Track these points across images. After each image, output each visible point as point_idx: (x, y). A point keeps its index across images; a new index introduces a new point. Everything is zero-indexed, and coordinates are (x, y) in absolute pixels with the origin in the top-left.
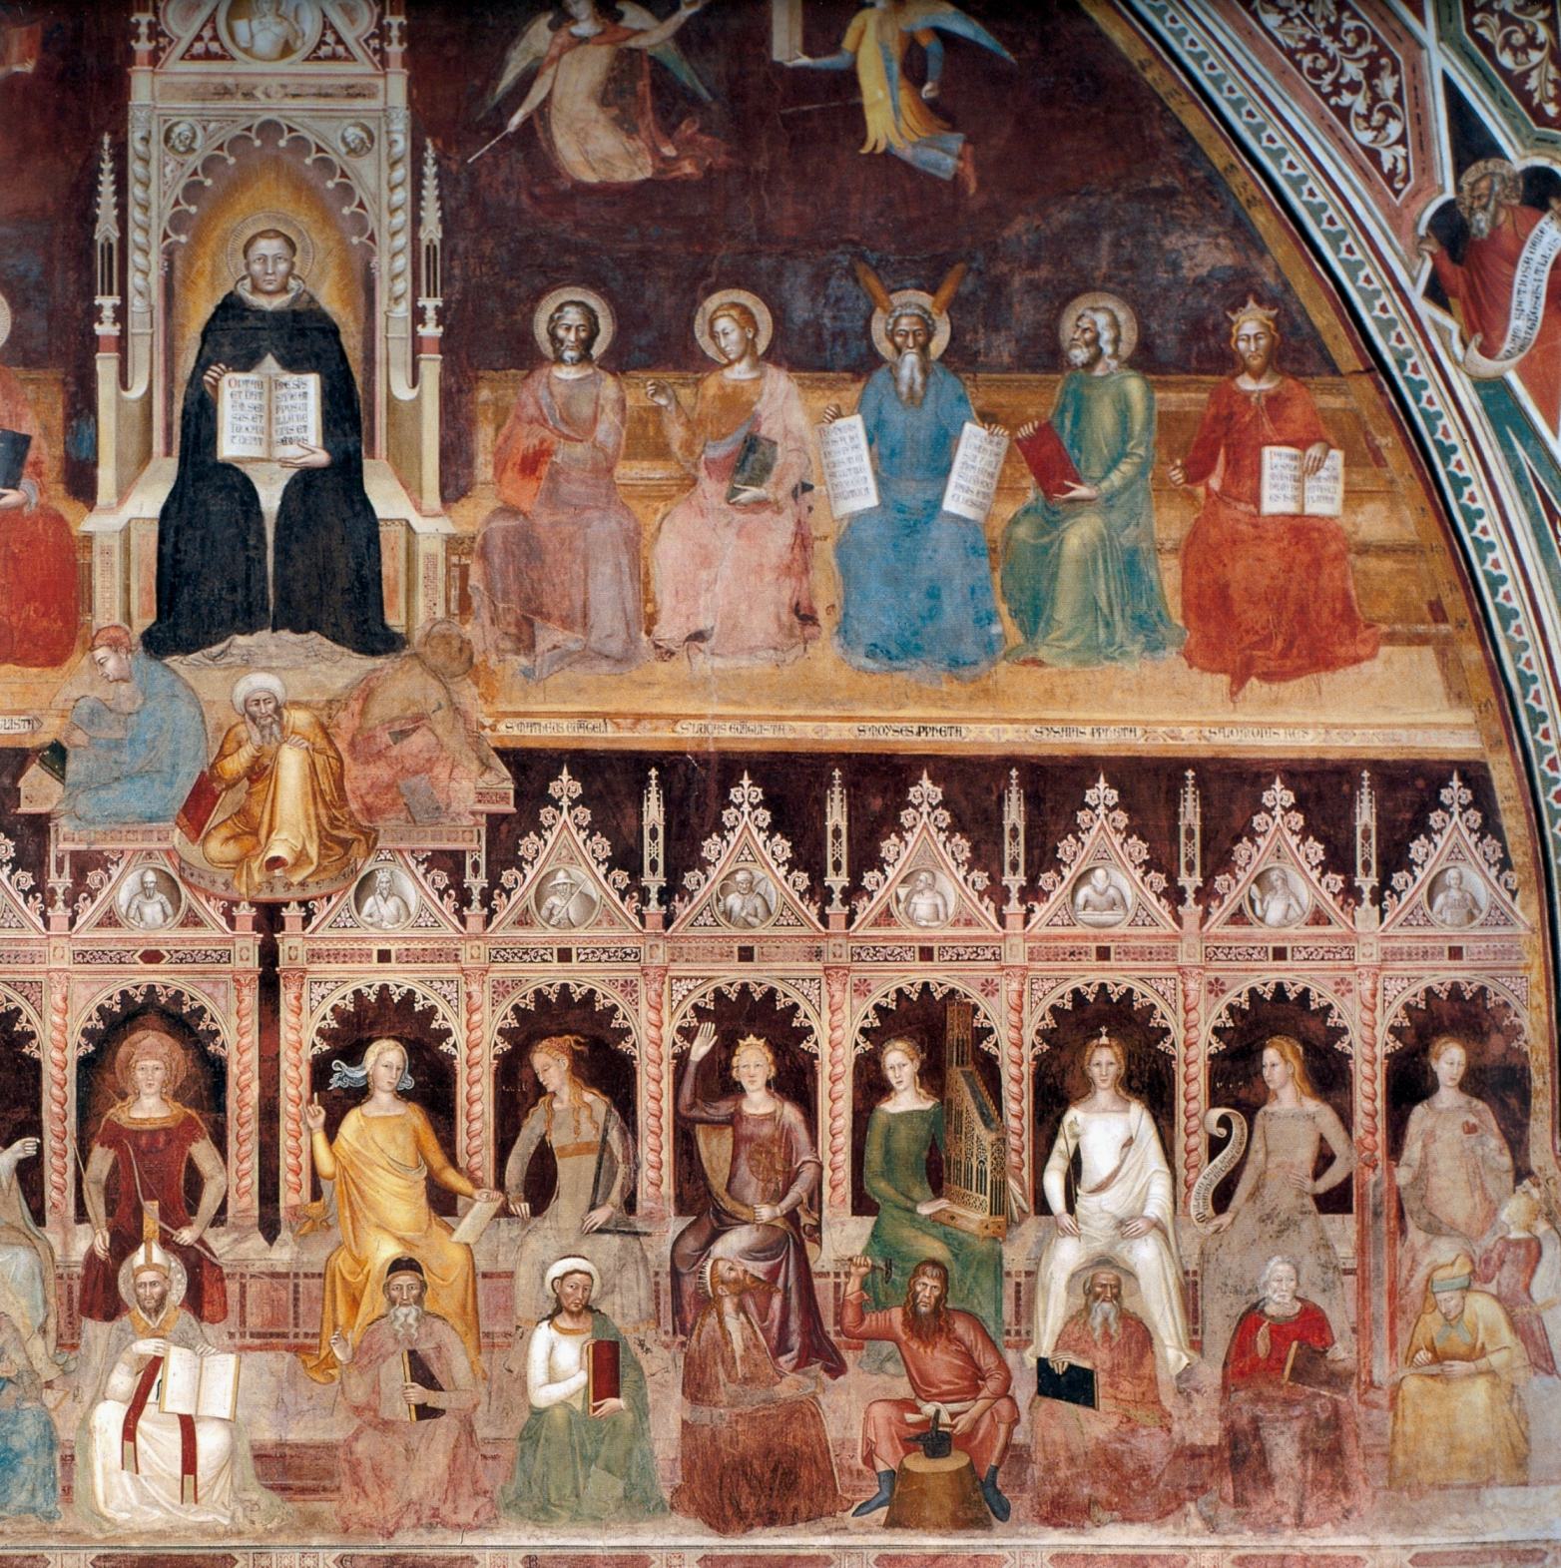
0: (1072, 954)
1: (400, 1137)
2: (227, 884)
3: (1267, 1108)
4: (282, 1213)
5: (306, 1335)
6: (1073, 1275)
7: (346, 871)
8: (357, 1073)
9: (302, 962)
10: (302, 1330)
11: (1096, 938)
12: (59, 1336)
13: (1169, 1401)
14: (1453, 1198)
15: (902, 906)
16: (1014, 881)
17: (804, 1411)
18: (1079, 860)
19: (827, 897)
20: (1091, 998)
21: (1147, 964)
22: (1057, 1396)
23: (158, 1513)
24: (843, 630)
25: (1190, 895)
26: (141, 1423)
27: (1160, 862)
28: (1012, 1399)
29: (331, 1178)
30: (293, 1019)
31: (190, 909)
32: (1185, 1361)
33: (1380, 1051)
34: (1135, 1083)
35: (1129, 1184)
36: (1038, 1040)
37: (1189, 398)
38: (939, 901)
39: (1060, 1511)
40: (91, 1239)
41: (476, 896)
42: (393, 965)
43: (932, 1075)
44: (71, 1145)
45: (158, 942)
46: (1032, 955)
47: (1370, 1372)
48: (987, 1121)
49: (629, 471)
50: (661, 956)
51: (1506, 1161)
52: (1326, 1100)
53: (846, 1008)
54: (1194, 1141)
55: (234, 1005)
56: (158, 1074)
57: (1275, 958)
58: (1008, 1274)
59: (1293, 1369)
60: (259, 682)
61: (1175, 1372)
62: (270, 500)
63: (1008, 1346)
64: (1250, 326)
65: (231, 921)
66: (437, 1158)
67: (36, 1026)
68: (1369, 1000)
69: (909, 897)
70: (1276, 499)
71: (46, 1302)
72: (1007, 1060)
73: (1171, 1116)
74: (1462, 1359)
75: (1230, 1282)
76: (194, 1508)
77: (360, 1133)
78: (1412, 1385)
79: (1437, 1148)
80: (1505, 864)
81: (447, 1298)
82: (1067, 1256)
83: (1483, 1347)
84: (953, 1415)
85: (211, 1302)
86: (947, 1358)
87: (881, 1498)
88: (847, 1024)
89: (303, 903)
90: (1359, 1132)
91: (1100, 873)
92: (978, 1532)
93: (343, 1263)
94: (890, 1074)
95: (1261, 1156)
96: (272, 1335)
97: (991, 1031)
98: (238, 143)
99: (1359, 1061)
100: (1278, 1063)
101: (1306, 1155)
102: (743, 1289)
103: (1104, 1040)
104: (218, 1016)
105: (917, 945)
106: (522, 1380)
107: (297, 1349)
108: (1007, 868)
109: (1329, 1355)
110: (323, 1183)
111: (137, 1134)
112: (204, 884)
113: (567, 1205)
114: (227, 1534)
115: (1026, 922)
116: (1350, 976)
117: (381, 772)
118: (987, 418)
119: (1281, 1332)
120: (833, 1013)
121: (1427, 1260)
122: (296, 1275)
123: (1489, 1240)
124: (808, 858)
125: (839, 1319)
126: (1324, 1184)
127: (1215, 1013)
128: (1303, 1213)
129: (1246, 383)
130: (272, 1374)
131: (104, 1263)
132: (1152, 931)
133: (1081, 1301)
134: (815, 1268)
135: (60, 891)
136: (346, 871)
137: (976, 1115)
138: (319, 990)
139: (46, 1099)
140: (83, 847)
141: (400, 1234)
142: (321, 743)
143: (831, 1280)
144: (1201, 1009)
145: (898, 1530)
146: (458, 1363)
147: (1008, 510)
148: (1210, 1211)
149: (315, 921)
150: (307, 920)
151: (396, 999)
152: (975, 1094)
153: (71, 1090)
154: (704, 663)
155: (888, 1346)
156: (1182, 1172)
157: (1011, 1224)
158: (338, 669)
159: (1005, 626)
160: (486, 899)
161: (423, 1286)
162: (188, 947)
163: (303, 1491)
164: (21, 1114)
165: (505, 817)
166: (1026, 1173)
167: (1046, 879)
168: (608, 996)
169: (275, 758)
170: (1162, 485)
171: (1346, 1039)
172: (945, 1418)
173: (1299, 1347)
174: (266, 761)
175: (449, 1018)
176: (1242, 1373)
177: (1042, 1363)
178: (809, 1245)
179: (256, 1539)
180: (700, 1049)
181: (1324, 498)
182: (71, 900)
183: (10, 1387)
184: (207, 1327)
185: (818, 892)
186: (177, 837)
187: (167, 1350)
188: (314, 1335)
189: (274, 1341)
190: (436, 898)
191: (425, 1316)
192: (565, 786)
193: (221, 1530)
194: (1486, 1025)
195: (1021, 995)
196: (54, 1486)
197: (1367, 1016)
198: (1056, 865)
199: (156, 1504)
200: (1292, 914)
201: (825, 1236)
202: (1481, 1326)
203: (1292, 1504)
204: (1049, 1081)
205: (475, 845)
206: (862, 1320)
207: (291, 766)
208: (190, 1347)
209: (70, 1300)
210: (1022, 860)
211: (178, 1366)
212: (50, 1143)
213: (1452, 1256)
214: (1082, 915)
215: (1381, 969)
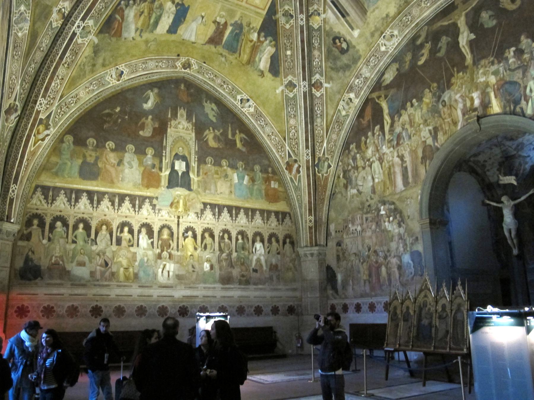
7: (187, 213)
14: (288, 254)
16: (250, 220)
17: (231, 273)
24: (235, 194)
26: (164, 271)
27: (263, 219)
37: (265, 176)
39: (255, 284)
40: (158, 251)
43: (243, 239)
46: (252, 227)
49: (215, 176)
50: (217, 225)
60: (178, 193)
62: (180, 174)
64: (270, 169)
70: (272, 186)
81: (196, 259)
82: (255, 258)
93: (185, 255)
98: (178, 137)
100: (273, 240)
101: (276, 249)
102: (226, 260)
106: (203, 268)
107: (180, 264)
113: (208, 250)
118: (248, 175)
119: (274, 266)
124: (231, 216)
129: (270, 175)
136: (187, 213)
146: (197, 266)
147: (249, 184)
154: (222, 195)
158: (187, 192)
159: (249, 195)
168: (212, 228)
170: (263, 184)
175: (197, 229)
180: (221, 235)
181: (276, 186)
182: (158, 214)
184: (171, 261)
185: (232, 219)
186: (169, 208)
192: (208, 206)
207: (181, 202)
211: (168, 265)
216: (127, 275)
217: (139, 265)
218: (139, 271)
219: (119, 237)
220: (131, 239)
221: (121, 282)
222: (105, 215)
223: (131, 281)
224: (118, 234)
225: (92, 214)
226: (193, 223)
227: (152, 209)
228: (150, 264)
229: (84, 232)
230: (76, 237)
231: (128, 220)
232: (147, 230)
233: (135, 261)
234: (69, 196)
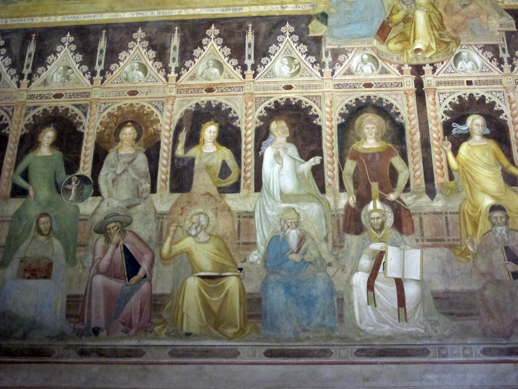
1: (487, 154)
2: (398, 59)
4: (436, 186)
5: (454, 240)
8: (463, 128)
9: (433, 85)
10: (451, 238)
12: (334, 242)
23: (387, 327)
26: (377, 283)
29: (457, 171)
30: (432, 108)
31: (383, 68)
41: (505, 60)
42: (474, 86)
44: (336, 159)
45: (370, 80)
55: (405, 102)
56: (374, 130)
65: (401, 72)
66: (505, 162)
67: (319, 112)
71: (327, 226)
76: (405, 324)
77: (468, 152)
85: (406, 226)
89: (432, 65)
93: (467, 207)
96: (437, 240)
104: (399, 107)
110: (454, 173)
111: (366, 155)
112: (388, 59)
114: (424, 337)
117: (458, 18)
122: (446, 213)
130: (439, 258)
131: (354, 210)
135: (327, 63)
138: (442, 97)
139: (324, 141)
140: (336, 47)
141: (492, 194)
142: (431, 9)
149: (437, 71)
150: (434, 71)
151: (477, 99)
153: (335, 137)
160: (510, 61)
161: (507, 217)
162: (383, 82)
163: (459, 315)
164: (313, 147)
165: (513, 32)
169: (414, 15)
174: (410, 16)
179: (440, 340)
183: (311, 266)
184: (406, 238)
186: (375, 43)
187: (386, 248)
188: (458, 240)
189: (439, 243)
190: (488, 61)
191: (509, 231)
193: (420, 335)
196: (334, 314)
199: (386, 322)
205: (502, 42)
207: (421, 18)
208: (397, 246)
209: (339, 226)
212: (327, 159)
216: (215, 308)
217: (265, 260)
218: (265, 284)
219: (179, 159)
220: (231, 163)
221: (188, 335)
222: (133, 93)
223: (230, 331)
224: (180, 152)
225: (87, 95)
226: (479, 83)
227: (308, 54)
228: (312, 254)
229: (58, 154)
230: (25, 175)
231: (215, 98)
232: (291, 126)
233: (251, 245)
234: (16, 51)
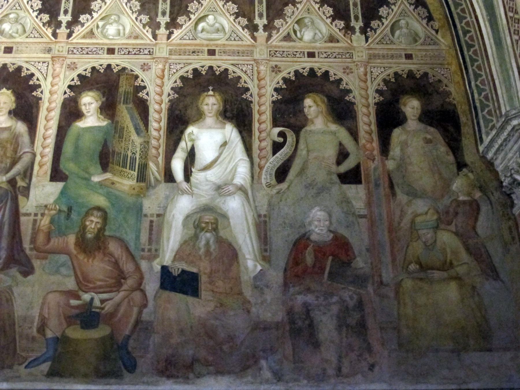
0: (194, 52)
3: (308, 128)
6: (188, 217)
11: (207, 45)
13: (248, 292)
15: (99, 30)
18: (199, 12)
19: (59, 24)
20: (204, 73)
21: (236, 58)
22: (174, 289)
25: (261, 28)
28: (143, 292)
32: (259, 268)
33: (372, 101)
34: (228, 114)
35: (224, 166)
36: (171, 92)
38: (121, 28)
47: (380, 276)
48: (138, 132)
51: (451, 158)
52: (342, 125)
53: (62, 76)
54: (264, 144)
57: (309, 57)
58: (146, 216)
59: (330, 273)
61: (252, 275)
63: (143, 258)
68: (363, 78)
69: (104, 26)
72: (153, 102)
73: (250, 131)
74: (438, 269)
75: (287, 221)
78: (408, 284)
79: (410, 150)
80: (430, 18)
83: (451, 263)
84: (102, 301)
86: (102, 265)
87: (47, 356)
88: (60, 84)
90: (362, 141)
91: (211, 17)
92: (113, 380)
94: (83, 109)
95: (304, 152)
97: (145, 87)
99: (360, 106)
101: (331, 153)
103: (211, 93)
105: (106, 47)
108: (160, 14)
109: (352, 265)
115: (169, 37)
116: (352, 65)
120: (54, 78)
121: (410, 212)
123: (446, 201)
125: (33, 240)
126: (344, 168)
127: (276, 80)
128: (331, 183)
132: (240, 43)
133: (192, 232)
134: (22, 210)
137: (132, 129)
143: (32, 218)
144: (268, 79)
145: (57, 379)
148: (274, 182)
152: (132, 118)
155: (63, 258)
156: (256, 160)
157: (149, 187)
166: (161, 160)
167: (181, 20)
171: (351, 95)
172: (97, 303)
173: (333, 260)
176: (297, 276)
177: (164, 269)
178: (20, 198)
194: (430, 91)
195: (163, 71)
197: (362, 84)
198: (187, 13)
200: (317, 37)
201: (33, 192)
202: (448, 250)
203: (334, 360)
204: (177, 112)
206: (49, 240)
210: (168, 11)
213: (426, 209)
214: (200, 35)
215: (368, 62)
